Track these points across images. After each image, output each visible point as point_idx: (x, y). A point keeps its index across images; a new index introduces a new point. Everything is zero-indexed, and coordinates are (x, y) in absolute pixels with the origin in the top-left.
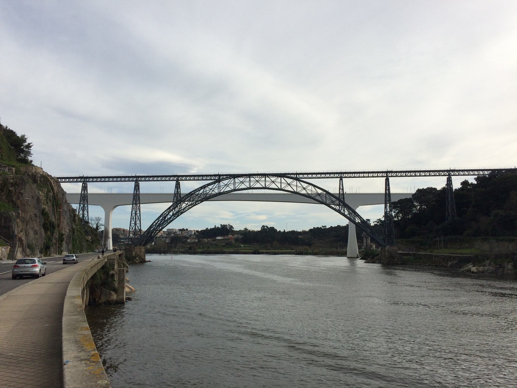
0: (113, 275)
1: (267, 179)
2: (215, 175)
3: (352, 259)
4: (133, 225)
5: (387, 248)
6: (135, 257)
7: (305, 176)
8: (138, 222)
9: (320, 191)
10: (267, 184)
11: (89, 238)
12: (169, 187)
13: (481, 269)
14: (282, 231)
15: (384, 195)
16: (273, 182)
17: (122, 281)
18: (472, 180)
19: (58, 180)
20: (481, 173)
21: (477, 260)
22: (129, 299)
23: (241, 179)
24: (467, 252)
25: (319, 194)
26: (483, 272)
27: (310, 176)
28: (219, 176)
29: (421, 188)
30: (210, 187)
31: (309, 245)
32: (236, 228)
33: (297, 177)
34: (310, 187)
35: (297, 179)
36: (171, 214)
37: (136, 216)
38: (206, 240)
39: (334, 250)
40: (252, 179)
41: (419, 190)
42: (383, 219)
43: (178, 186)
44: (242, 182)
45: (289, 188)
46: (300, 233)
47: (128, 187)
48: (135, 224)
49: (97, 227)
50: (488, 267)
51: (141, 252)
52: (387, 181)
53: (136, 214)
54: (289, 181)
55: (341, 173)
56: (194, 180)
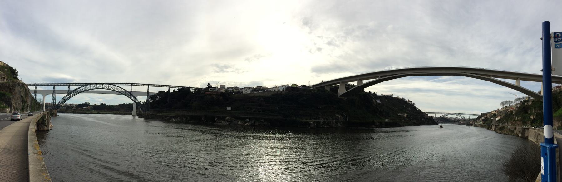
0: (45, 120)
1: (103, 85)
2: (84, 84)
3: (134, 116)
4: (53, 102)
5: (147, 112)
6: (53, 114)
7: (118, 84)
8: (55, 101)
9: (123, 90)
10: (103, 87)
11: (37, 106)
12: (66, 88)
13: (177, 120)
14: (108, 105)
15: (147, 93)
16: (105, 86)
17: (48, 123)
18: (176, 89)
19: (27, 85)
20: (179, 87)
21: (175, 117)
22: (51, 130)
23: (94, 85)
24: (173, 114)
25: (123, 91)
26: (177, 121)
27: (120, 84)
28: (85, 84)
29: (160, 91)
30: (82, 88)
31: (118, 110)
32: (91, 104)
33: (115, 84)
34: (120, 88)
35: (115, 85)
36: (67, 98)
37: (54, 98)
38: (79, 108)
39: (127, 112)
40: (98, 85)
41: (159, 92)
42: (146, 102)
43: (69, 87)
44: (94, 86)
45: (112, 89)
46: (115, 106)
47: (51, 88)
48: (54, 101)
49: (40, 102)
50: (179, 120)
51: (55, 112)
52: (148, 87)
53: (54, 98)
54: (112, 86)
55: (132, 84)
56: (76, 85)
